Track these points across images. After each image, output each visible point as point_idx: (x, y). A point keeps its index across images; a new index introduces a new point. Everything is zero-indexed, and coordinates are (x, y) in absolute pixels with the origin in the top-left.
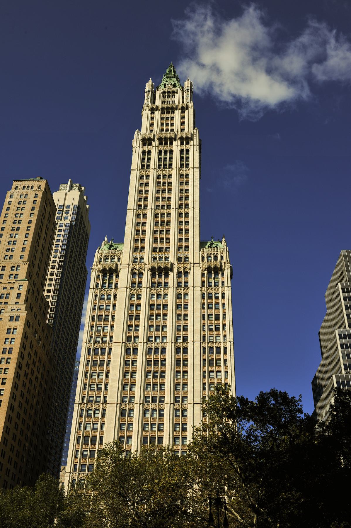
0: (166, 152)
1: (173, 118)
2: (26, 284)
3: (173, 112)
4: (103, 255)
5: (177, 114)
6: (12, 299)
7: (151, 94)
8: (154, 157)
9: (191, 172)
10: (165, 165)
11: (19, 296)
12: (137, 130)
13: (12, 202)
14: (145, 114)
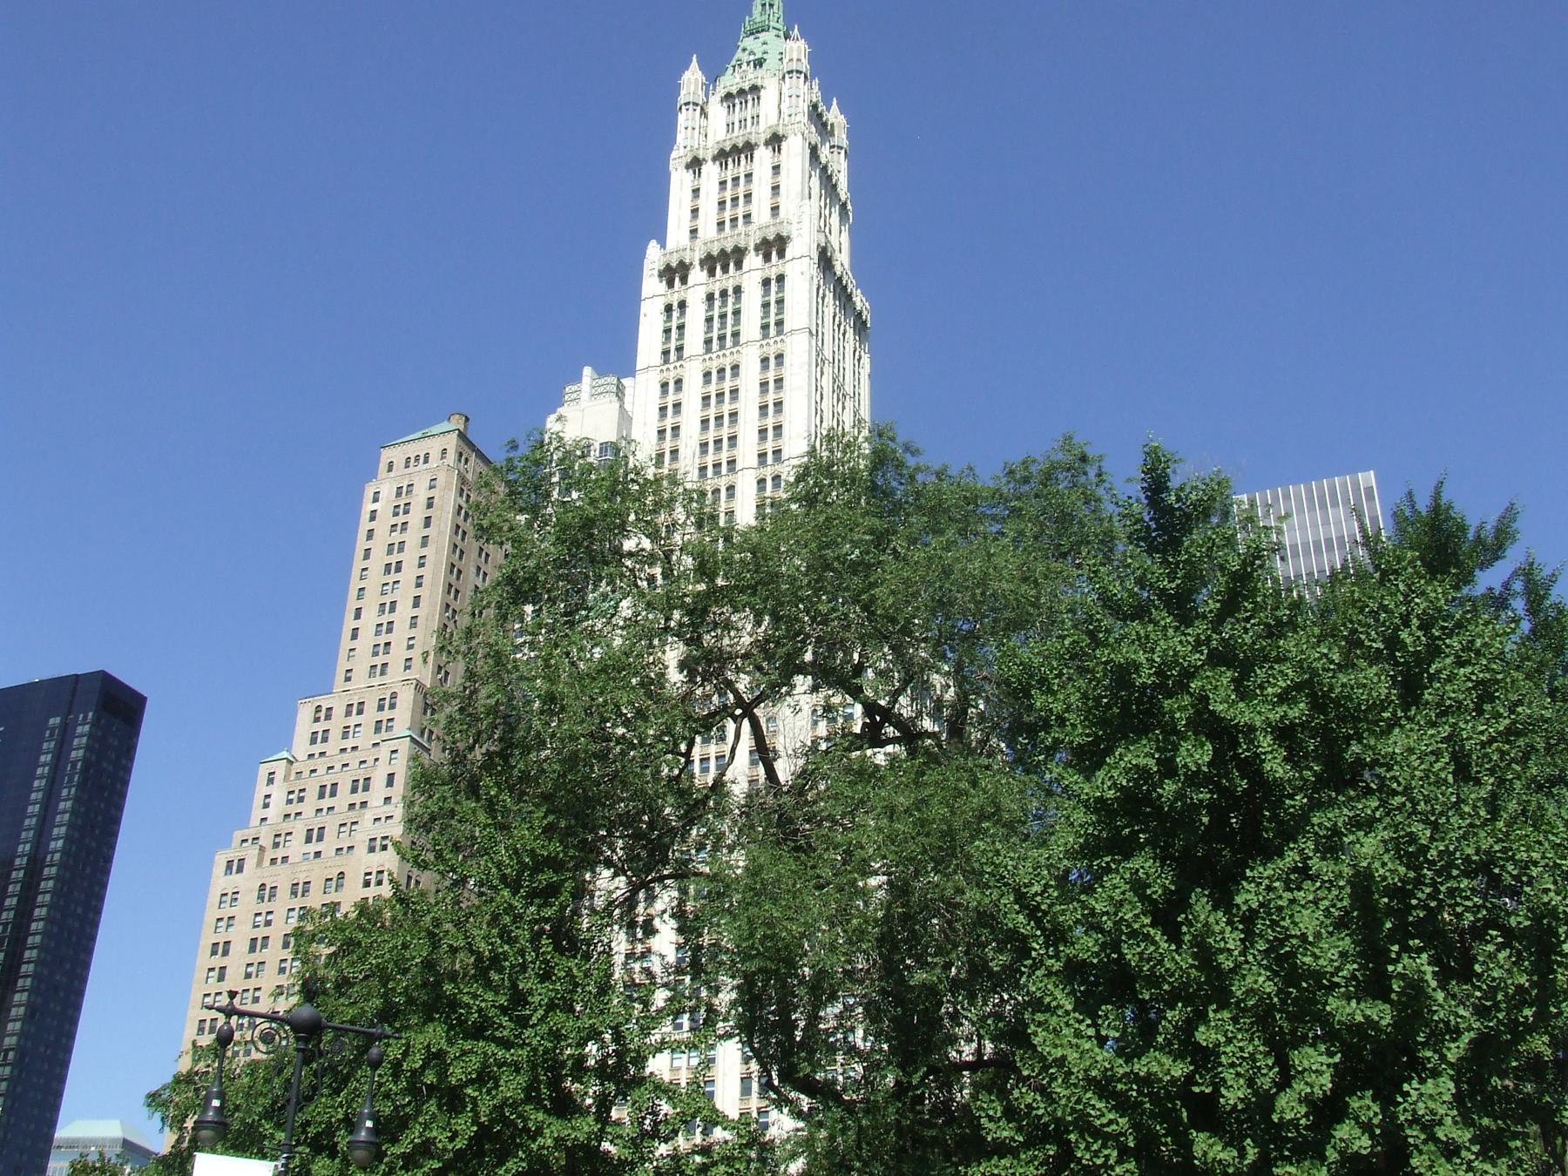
2: (405, 747)
6: (378, 790)
8: (695, 317)
10: (722, 338)
14: (680, 180)
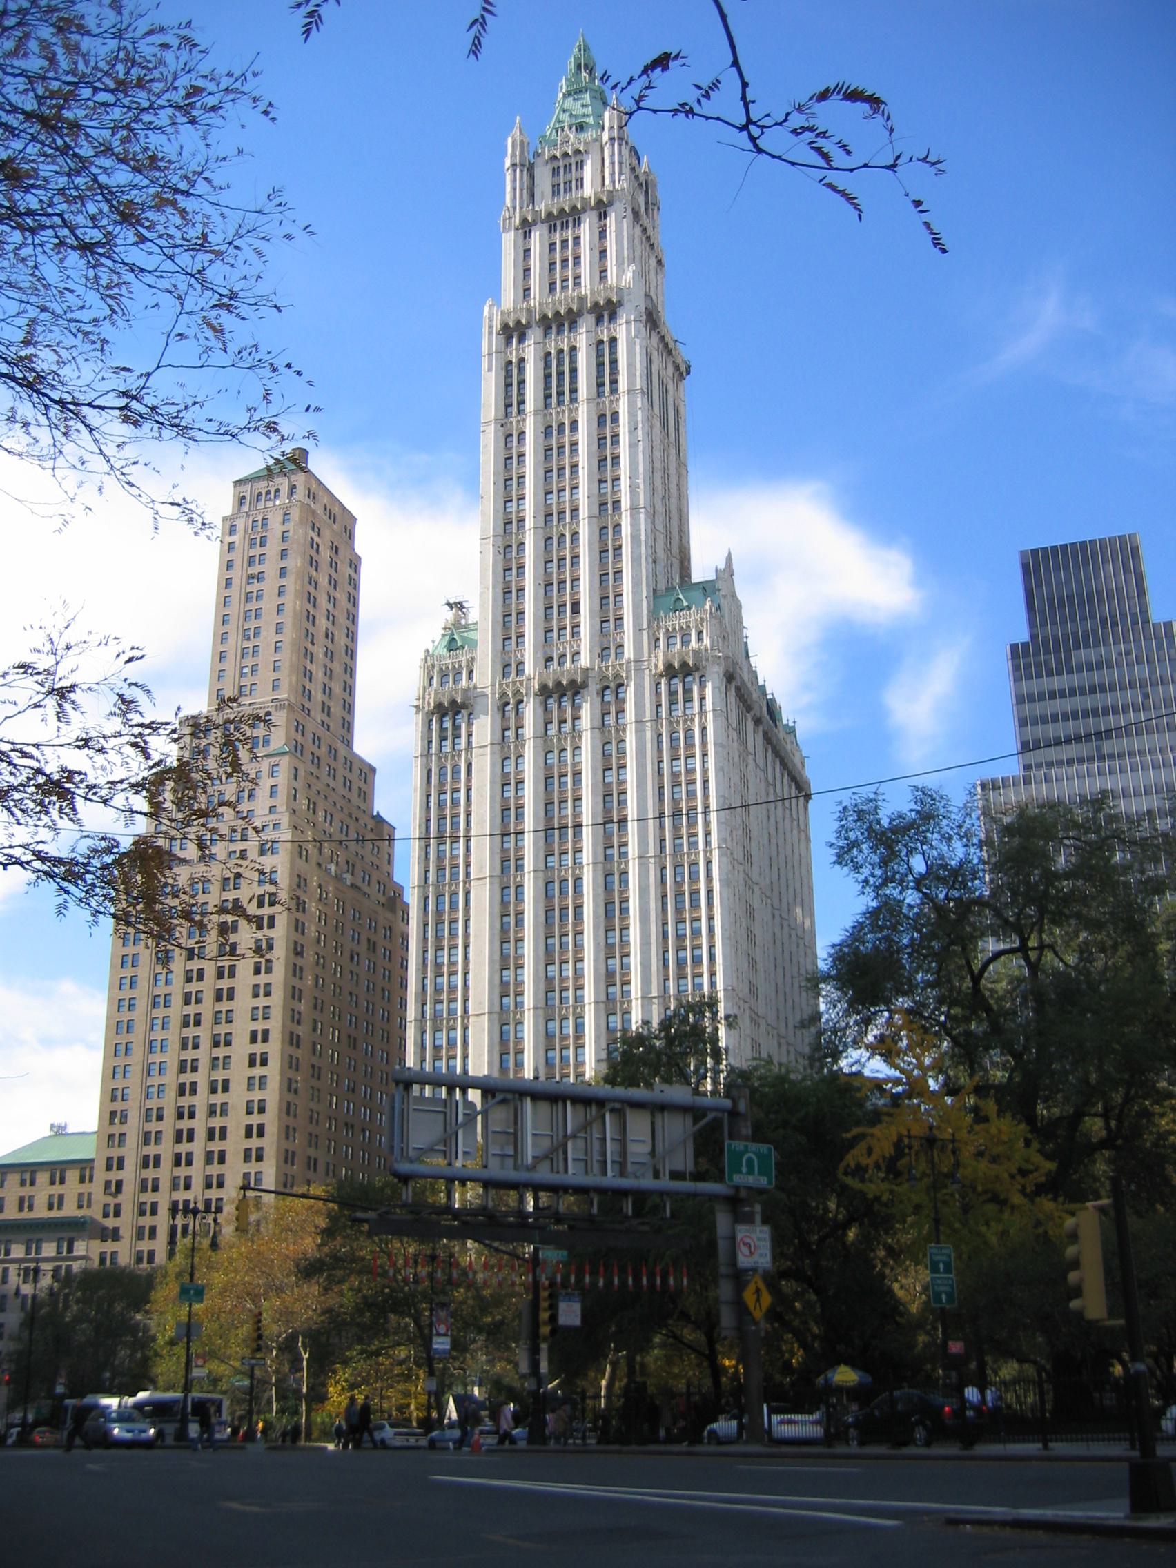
0: (561, 351)
1: (577, 240)
3: (577, 223)
4: (436, 669)
5: (586, 230)
7: (522, 171)
9: (623, 408)
10: (560, 394)
11: (273, 791)
12: (489, 302)
13: (237, 544)
